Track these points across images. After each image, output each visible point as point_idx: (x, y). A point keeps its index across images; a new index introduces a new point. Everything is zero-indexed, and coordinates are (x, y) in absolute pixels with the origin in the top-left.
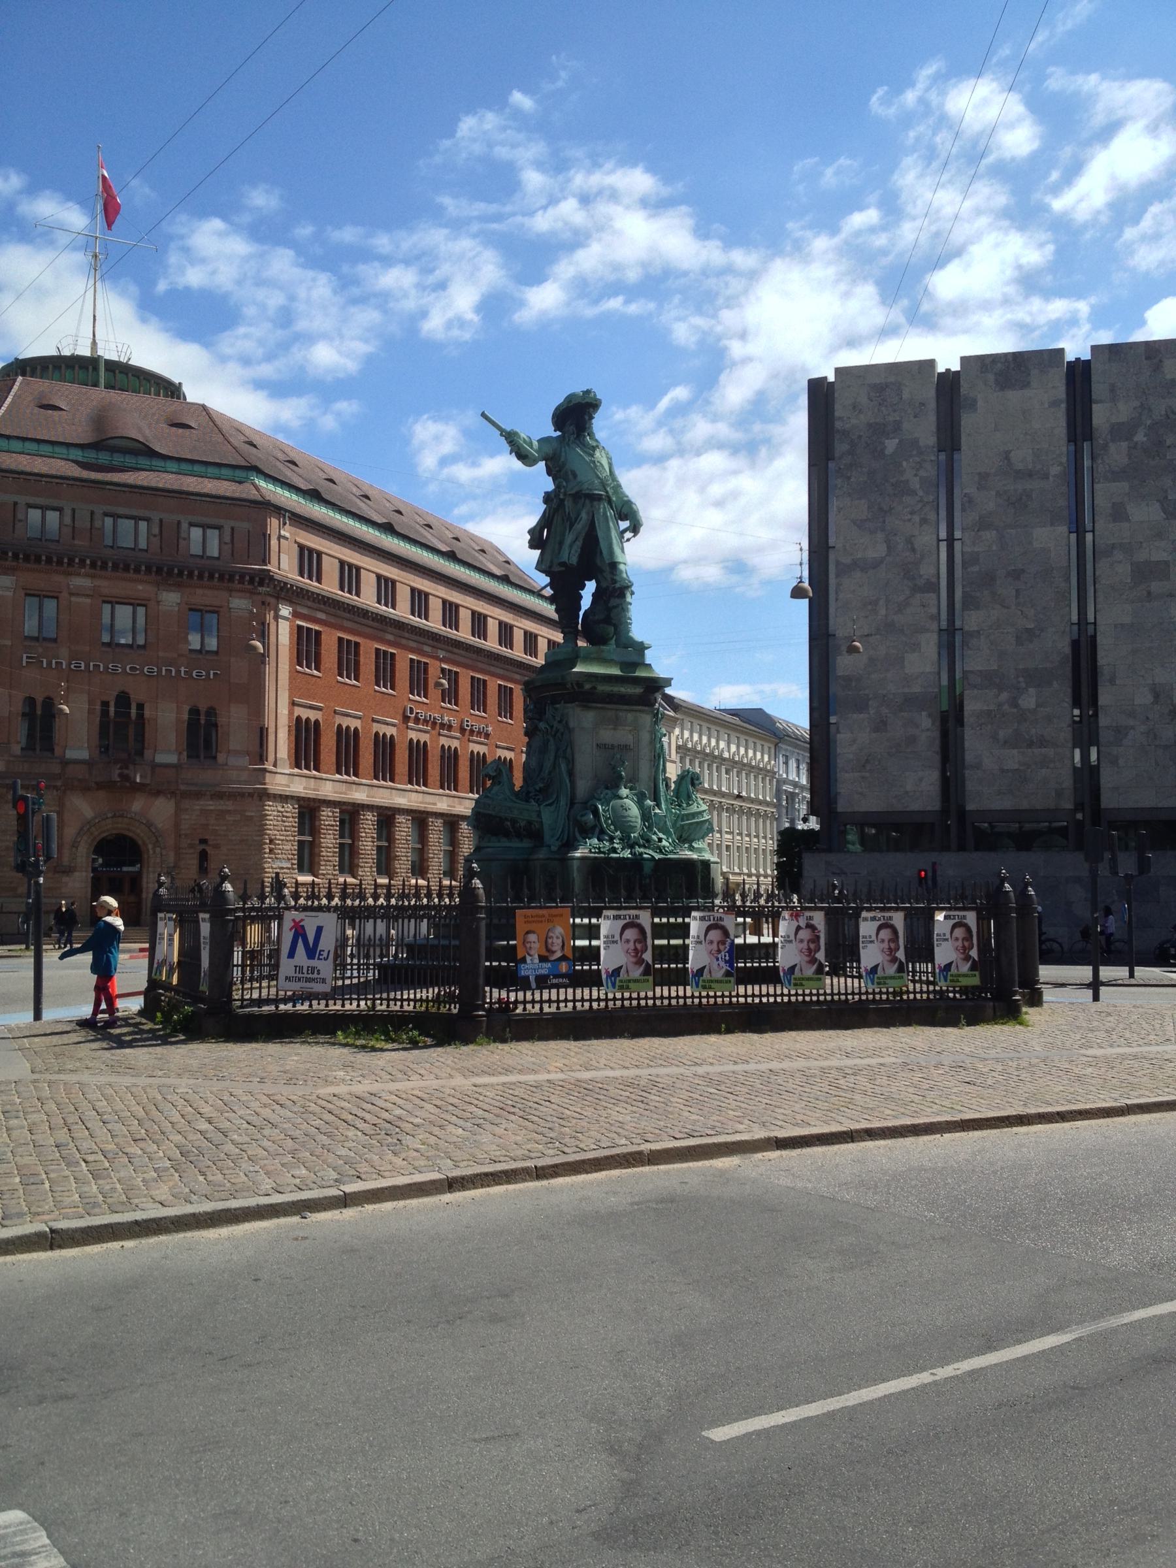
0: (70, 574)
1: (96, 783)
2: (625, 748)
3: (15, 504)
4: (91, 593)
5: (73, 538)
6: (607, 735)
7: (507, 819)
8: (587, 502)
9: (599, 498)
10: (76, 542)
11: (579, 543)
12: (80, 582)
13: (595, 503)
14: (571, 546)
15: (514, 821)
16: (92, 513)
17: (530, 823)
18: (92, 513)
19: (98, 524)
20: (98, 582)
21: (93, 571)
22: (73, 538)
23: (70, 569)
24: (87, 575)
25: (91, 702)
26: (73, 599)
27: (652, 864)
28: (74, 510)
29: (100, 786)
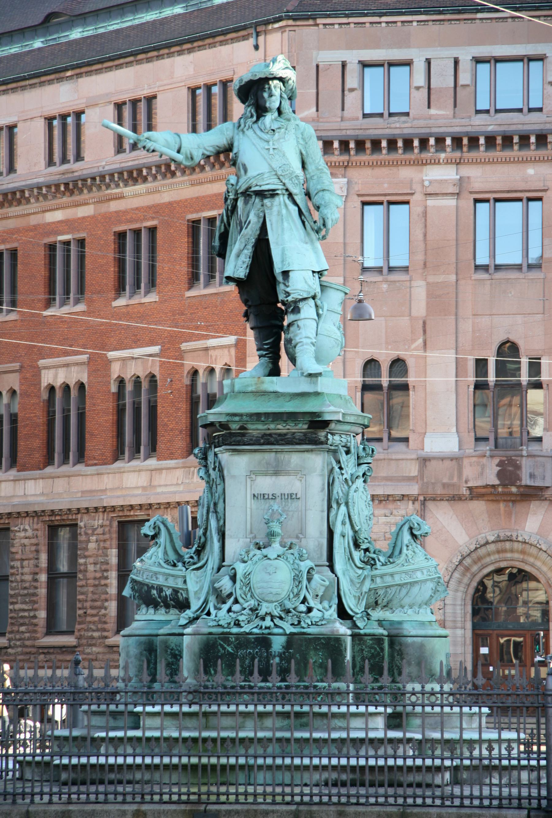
0: (424, 163)
1: (470, 488)
2: (292, 497)
3: (344, 65)
4: (451, 189)
5: (429, 107)
6: (265, 484)
7: (153, 587)
8: (257, 200)
9: (273, 194)
10: (433, 111)
11: (248, 251)
12: (441, 173)
13: (267, 201)
14: (238, 256)
15: (160, 589)
16: (456, 62)
17: (176, 591)
18: (456, 62)
19: (465, 78)
20: (467, 171)
21: (458, 154)
22: (429, 107)
23: (425, 155)
24: (448, 162)
25: (459, 364)
26: (431, 202)
27: (283, 639)
28: (428, 62)
29: (475, 494)
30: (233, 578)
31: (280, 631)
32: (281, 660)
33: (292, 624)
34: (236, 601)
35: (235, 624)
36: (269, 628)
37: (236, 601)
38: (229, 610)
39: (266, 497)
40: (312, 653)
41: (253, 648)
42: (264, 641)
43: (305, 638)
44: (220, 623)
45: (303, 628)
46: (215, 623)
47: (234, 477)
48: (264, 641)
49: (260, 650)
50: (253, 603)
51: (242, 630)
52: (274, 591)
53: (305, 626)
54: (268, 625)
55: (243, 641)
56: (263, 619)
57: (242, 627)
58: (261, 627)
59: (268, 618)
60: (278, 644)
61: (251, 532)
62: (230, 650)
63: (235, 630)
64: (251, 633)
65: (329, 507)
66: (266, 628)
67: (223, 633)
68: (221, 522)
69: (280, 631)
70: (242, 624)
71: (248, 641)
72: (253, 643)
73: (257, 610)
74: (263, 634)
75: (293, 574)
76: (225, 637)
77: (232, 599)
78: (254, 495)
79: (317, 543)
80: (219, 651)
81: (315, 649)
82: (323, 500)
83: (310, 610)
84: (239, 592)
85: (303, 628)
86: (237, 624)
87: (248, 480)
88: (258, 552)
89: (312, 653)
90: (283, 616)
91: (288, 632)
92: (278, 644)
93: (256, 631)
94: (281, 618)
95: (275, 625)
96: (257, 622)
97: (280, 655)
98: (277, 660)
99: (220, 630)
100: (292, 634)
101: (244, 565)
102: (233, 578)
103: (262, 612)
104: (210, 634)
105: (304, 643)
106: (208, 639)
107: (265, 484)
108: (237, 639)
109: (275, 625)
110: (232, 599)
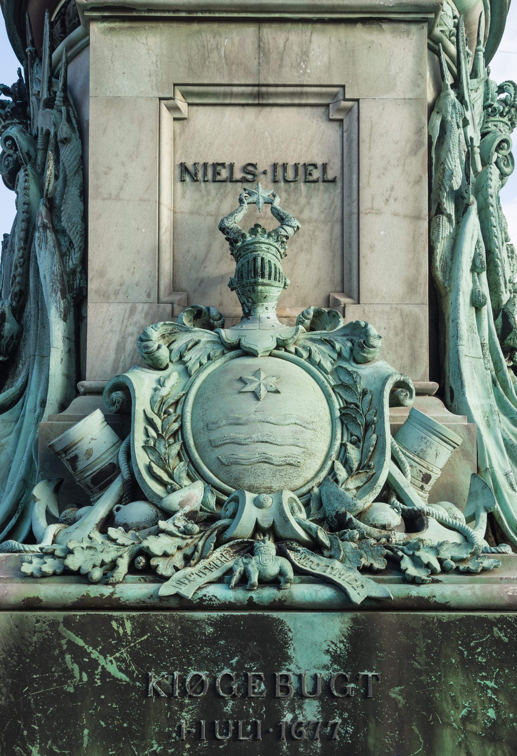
6: (226, 134)
27: (332, 629)
30: (120, 421)
31: (324, 593)
32: (327, 712)
33: (366, 570)
34: (134, 492)
35: (132, 569)
36: (276, 581)
37: (134, 492)
38: (108, 522)
39: (224, 173)
40: (455, 681)
41: (212, 663)
42: (255, 634)
43: (427, 622)
44: (73, 562)
45: (415, 581)
46: (50, 566)
47: (115, 102)
48: (255, 634)
49: (239, 667)
50: (192, 495)
51: (166, 590)
52: (275, 453)
53: (422, 574)
54: (272, 570)
55: (169, 629)
56: (247, 549)
57: (164, 579)
58: (244, 579)
59: (269, 546)
60: (313, 644)
61: (175, 288)
62: (113, 669)
63: (135, 590)
64: (202, 605)
65: (436, 210)
66: (265, 582)
67: (83, 604)
68: (75, 258)
69: (324, 593)
70: (163, 567)
71: (189, 630)
72: (212, 641)
73: (212, 518)
74: (251, 605)
75: (337, 404)
76: (95, 615)
77: (115, 488)
78: (184, 169)
79: (396, 320)
80: (68, 674)
81: (469, 666)
82: (418, 181)
83: (414, 521)
84: (142, 459)
85: (415, 581)
86: (143, 566)
87: (167, 116)
88: (205, 336)
89: (455, 681)
90: (323, 536)
91: (357, 598)
92: (313, 644)
93: (221, 593)
94: (315, 546)
95: (298, 571)
96: (221, 558)
97: (327, 693)
98: (311, 711)
99: (73, 591)
100: (373, 604)
101: (156, 375)
102: (120, 421)
103: (244, 526)
104: (32, 605)
105: (422, 644)
106: (20, 625)
107: (226, 134)
108: (141, 628)
109: (298, 571)
110: (115, 488)
